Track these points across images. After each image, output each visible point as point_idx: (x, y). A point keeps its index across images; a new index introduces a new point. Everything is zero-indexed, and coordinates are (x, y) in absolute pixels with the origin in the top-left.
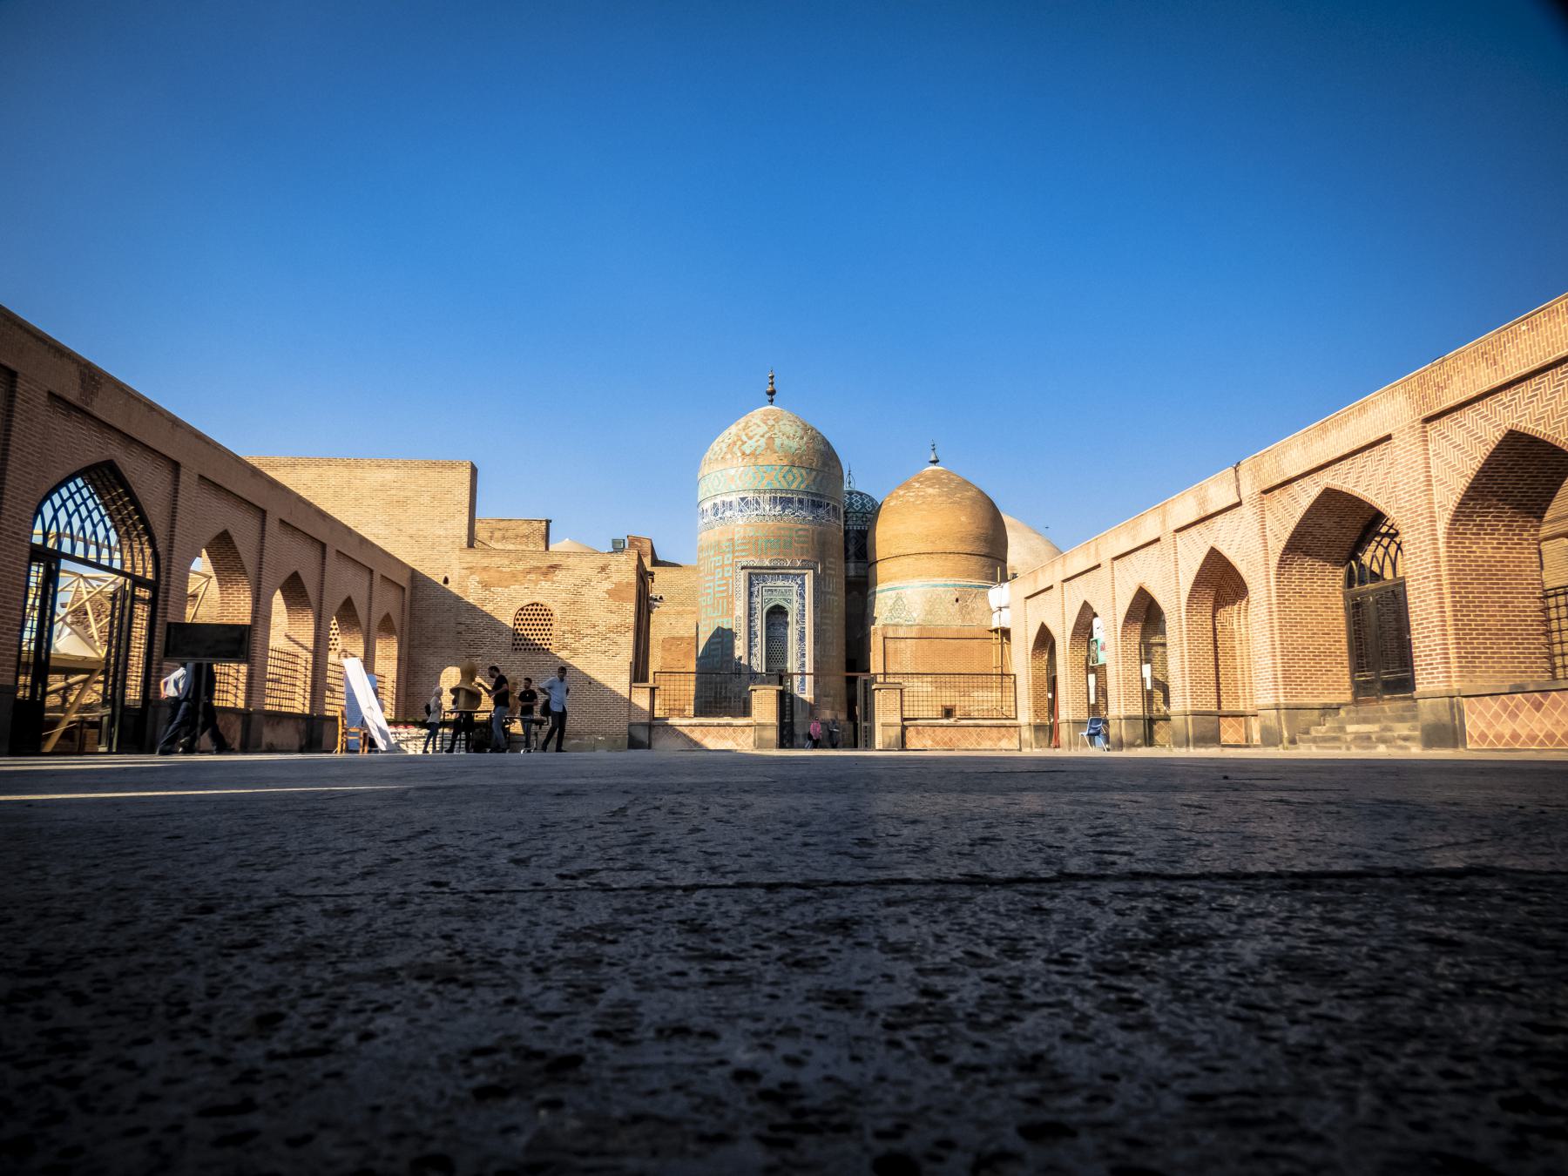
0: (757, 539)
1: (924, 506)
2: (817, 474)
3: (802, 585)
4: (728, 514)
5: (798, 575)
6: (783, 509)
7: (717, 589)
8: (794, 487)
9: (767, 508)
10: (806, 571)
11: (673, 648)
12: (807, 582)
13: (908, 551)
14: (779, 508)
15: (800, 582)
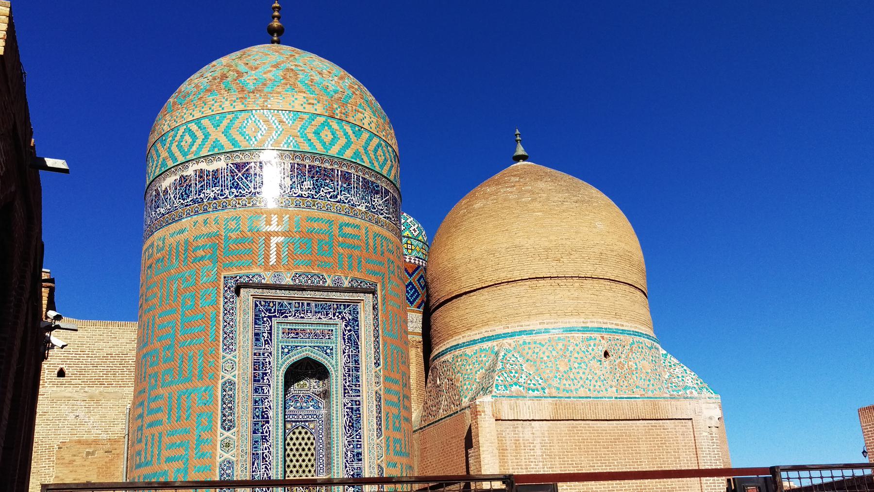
1: (537, 205)
2: (370, 140)
3: (353, 323)
4: (210, 192)
6: (317, 187)
8: (334, 151)
10: (361, 296)
11: (79, 461)
12: (362, 317)
13: (517, 275)
14: (308, 184)
15: (348, 317)
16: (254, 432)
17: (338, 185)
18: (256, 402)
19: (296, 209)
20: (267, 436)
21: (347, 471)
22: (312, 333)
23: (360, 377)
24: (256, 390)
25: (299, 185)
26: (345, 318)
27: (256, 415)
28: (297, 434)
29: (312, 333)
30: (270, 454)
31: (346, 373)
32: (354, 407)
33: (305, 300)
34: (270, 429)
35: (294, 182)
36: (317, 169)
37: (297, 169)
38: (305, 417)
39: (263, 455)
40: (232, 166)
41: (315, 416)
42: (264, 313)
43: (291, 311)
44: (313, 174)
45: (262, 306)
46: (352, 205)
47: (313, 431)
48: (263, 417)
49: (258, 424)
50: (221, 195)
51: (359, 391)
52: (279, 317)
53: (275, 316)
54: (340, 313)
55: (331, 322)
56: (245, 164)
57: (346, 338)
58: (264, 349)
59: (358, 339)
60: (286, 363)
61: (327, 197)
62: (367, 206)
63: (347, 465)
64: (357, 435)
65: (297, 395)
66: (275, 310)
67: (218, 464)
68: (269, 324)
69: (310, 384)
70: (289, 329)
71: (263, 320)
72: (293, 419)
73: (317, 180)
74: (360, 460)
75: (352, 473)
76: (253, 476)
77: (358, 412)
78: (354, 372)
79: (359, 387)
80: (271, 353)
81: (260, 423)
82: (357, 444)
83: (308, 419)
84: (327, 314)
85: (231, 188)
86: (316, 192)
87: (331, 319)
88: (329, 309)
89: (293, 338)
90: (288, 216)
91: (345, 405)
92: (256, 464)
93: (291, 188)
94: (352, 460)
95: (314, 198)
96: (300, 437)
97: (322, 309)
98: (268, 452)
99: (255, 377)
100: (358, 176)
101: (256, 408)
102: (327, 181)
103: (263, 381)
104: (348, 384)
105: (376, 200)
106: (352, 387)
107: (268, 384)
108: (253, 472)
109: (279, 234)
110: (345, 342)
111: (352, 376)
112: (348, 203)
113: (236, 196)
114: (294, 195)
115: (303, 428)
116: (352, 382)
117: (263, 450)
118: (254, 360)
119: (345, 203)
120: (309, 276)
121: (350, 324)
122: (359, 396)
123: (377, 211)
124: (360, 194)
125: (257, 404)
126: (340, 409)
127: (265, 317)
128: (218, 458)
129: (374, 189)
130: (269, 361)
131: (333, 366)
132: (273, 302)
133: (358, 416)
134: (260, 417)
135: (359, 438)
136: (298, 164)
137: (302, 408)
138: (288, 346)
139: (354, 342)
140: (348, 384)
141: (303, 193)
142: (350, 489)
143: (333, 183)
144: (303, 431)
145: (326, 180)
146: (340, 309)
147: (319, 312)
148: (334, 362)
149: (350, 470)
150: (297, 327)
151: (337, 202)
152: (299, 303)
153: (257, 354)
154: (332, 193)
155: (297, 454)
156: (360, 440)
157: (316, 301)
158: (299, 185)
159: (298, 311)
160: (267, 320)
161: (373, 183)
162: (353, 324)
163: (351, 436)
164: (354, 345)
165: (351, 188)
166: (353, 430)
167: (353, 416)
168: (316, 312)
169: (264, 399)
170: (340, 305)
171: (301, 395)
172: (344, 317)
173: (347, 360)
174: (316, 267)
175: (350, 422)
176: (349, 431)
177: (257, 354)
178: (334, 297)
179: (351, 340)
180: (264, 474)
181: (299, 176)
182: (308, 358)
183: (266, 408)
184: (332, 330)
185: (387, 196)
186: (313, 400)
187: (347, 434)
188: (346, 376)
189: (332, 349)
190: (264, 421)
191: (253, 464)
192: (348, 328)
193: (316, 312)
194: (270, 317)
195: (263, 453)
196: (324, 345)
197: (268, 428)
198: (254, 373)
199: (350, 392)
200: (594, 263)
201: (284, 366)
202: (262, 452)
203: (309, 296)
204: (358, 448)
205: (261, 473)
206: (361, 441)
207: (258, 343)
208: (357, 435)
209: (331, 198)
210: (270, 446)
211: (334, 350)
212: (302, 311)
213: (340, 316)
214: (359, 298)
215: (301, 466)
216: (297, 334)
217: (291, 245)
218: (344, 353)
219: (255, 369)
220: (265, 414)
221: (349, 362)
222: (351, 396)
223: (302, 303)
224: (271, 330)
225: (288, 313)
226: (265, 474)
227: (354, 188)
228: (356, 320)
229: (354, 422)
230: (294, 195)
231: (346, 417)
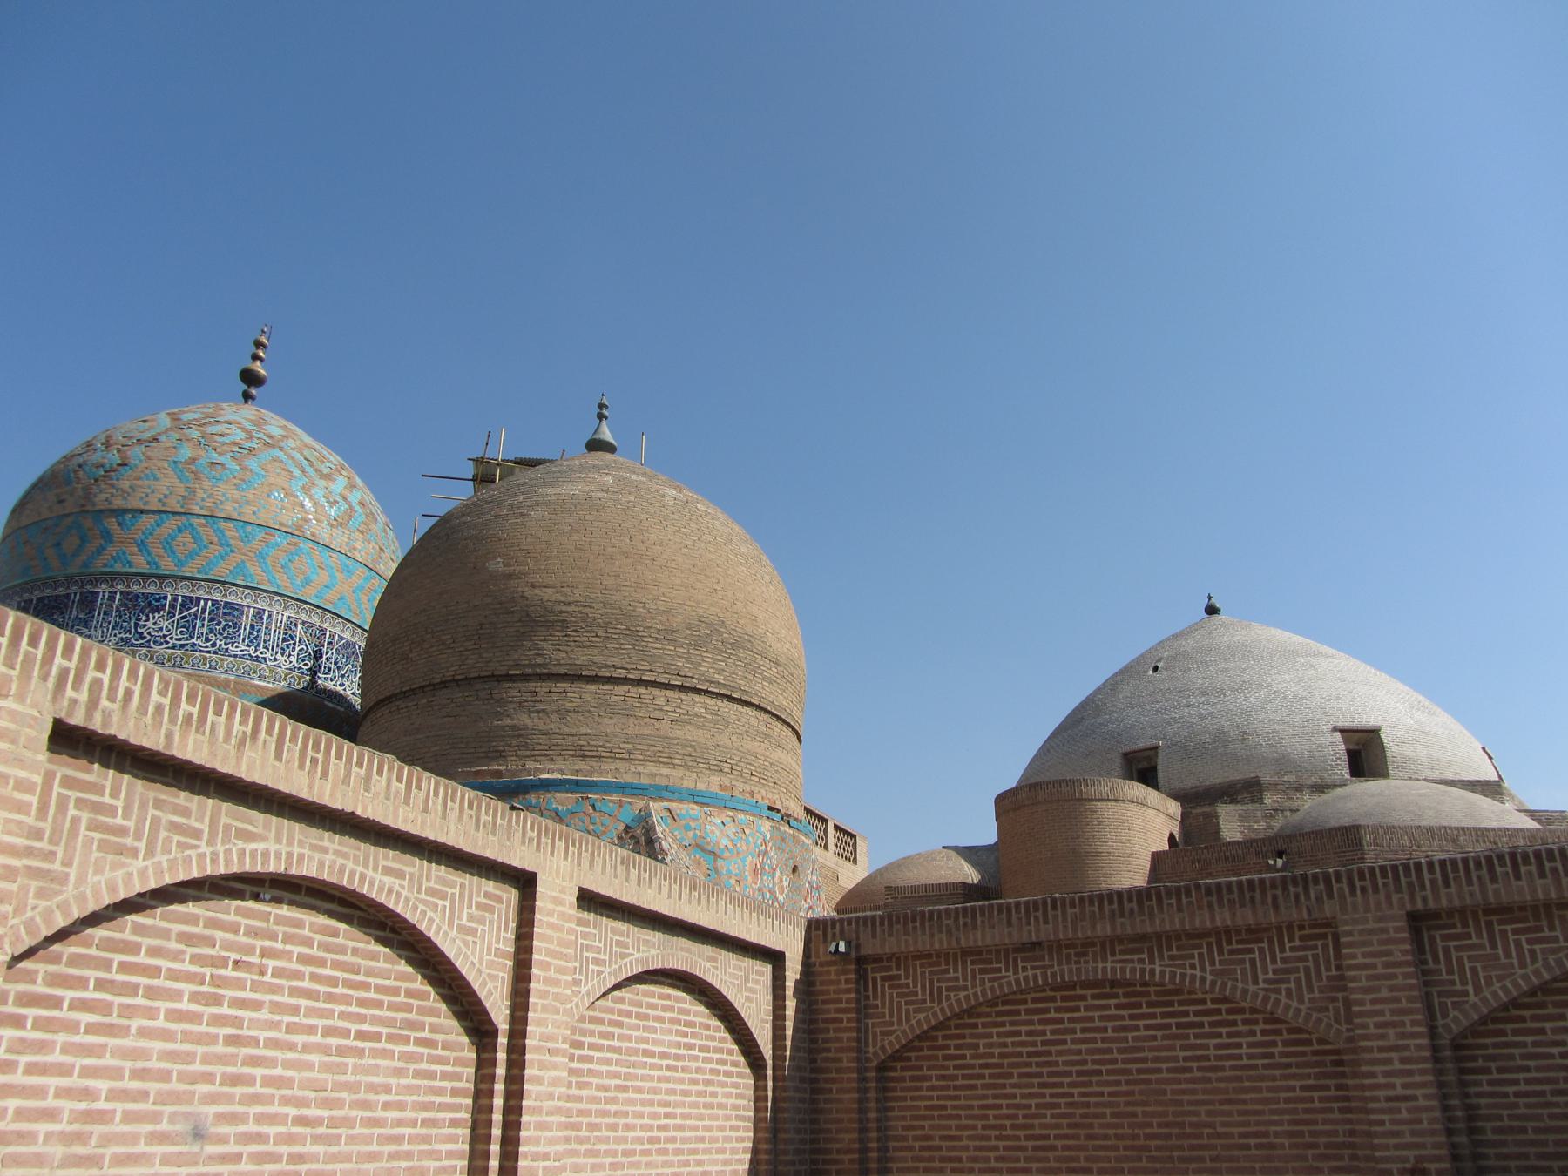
36: (46, 602)
62: (122, 639)
102: (55, 617)
105: (150, 624)
123: (149, 641)
124: (109, 623)
129: (150, 603)
165: (93, 617)
200: (461, 649)
227: (99, 614)
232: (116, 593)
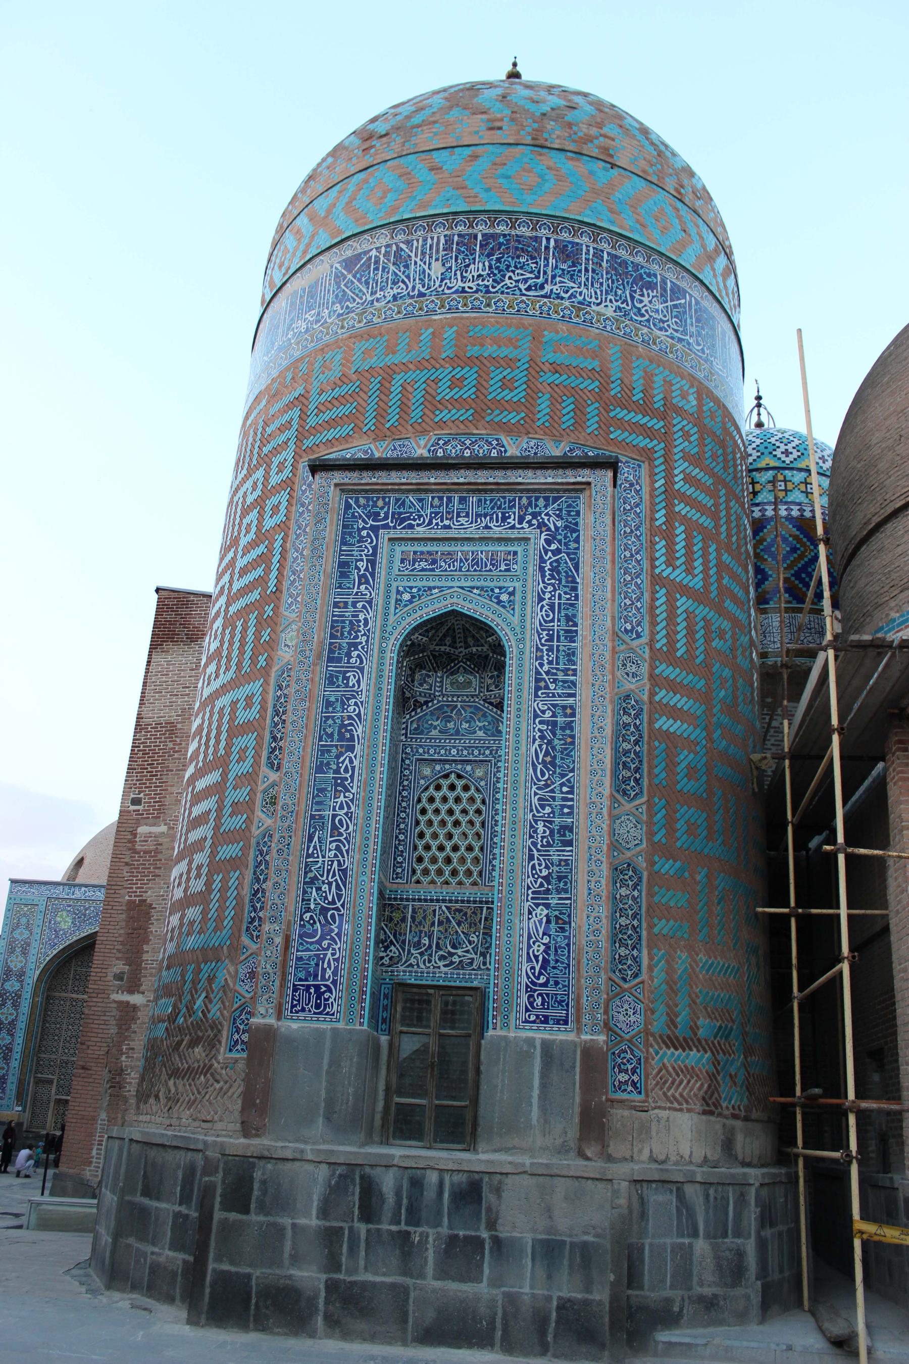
0: (389, 372)
5: (552, 493)
6: (497, 273)
7: (236, 586)
9: (436, 270)
10: (584, 475)
16: (319, 769)
17: (546, 266)
18: (329, 704)
19: (448, 316)
20: (346, 779)
21: (533, 867)
22: (467, 560)
23: (579, 652)
24: (331, 680)
25: (458, 273)
26: (546, 525)
27: (326, 733)
28: (445, 789)
29: (467, 560)
30: (350, 819)
31: (543, 645)
32: (560, 720)
33: (456, 491)
34: (356, 763)
35: (450, 268)
36: (501, 240)
37: (458, 244)
38: (465, 752)
39: (333, 820)
40: (338, 266)
41: (487, 752)
42: (364, 521)
43: (420, 516)
44: (492, 249)
45: (359, 507)
46: (579, 303)
47: (483, 783)
48: (341, 737)
49: (329, 751)
50: (317, 321)
51: (575, 685)
52: (395, 527)
53: (386, 527)
54: (535, 515)
55: (514, 534)
56: (358, 257)
57: (548, 566)
58: (357, 594)
59: (577, 570)
60: (404, 623)
61: (520, 290)
62: (619, 308)
63: (535, 852)
64: (562, 785)
65: (448, 706)
66: (387, 514)
67: (253, 841)
68: (372, 542)
69: (481, 682)
70: (415, 553)
71: (359, 535)
72: (436, 757)
73: (498, 260)
74: (570, 843)
75: (545, 873)
76: (306, 866)
77: (568, 732)
78: (564, 643)
79: (575, 675)
80: (370, 602)
81: (334, 750)
82: (563, 807)
83: (471, 758)
84: (504, 519)
85: (333, 303)
86: (494, 281)
87: (513, 527)
88: (510, 508)
89: (423, 570)
90: (431, 330)
91: (536, 716)
92: (316, 839)
93: (442, 280)
94: (548, 842)
95: (490, 292)
96: (451, 796)
97: (492, 508)
98: (346, 814)
99: (331, 651)
100: (598, 254)
101: (327, 718)
103: (348, 662)
104: (546, 668)
106: (556, 674)
107: (358, 668)
108: (308, 856)
109: (411, 366)
110: (543, 576)
111: (558, 651)
112: (569, 298)
113: (340, 315)
114: (446, 291)
115: (459, 777)
116: (558, 664)
117: (334, 810)
118: (333, 616)
119: (562, 298)
120: (468, 442)
121: (559, 537)
122: (574, 695)
123: (648, 321)
124: (602, 284)
125: (331, 709)
126: (524, 726)
127: (364, 528)
128: (253, 829)
129: (642, 278)
130: (366, 620)
131: (513, 629)
132: (384, 498)
133: (569, 740)
134: (336, 736)
135: (567, 793)
136: (459, 235)
137: (457, 732)
138: (411, 588)
139: (567, 576)
140: (546, 668)
141: (466, 285)
142: (538, 911)
143: (536, 263)
144: (459, 784)
145: (518, 257)
146: (536, 506)
147: (485, 516)
148: (516, 620)
149: (540, 865)
150: (435, 549)
151: (542, 296)
152: (441, 499)
153: (342, 605)
154: (530, 282)
155: (442, 833)
156: (570, 796)
157: (479, 491)
158: (458, 273)
159: (436, 514)
160: (368, 535)
161: (636, 266)
162: (566, 537)
163: (547, 786)
164: (567, 582)
165: (580, 271)
166: (554, 772)
167: (556, 742)
168: (478, 515)
169: (348, 699)
170: (537, 499)
171: (459, 704)
172: (543, 522)
173: (547, 616)
174: (480, 425)
175: (547, 753)
176: (543, 774)
177: (342, 605)
178: (520, 480)
179: (559, 573)
180: (333, 862)
181: (460, 257)
182: (454, 614)
183: (350, 718)
184: (515, 553)
185: (678, 299)
186: (484, 716)
187: (539, 780)
188: (542, 651)
189: (512, 594)
190: (342, 746)
191: (311, 839)
192: (553, 547)
193: (478, 515)
194: (375, 529)
195: (334, 816)
196: (492, 585)
197: (351, 761)
198: (331, 644)
199: (552, 686)
201: (399, 629)
202: (331, 812)
203: (462, 480)
204: (563, 814)
205: (327, 859)
206: (572, 800)
207: (345, 582)
208: (562, 785)
209: (527, 290)
210: (352, 800)
211: (518, 597)
212: (448, 513)
213: (534, 522)
214: (579, 479)
215: (448, 860)
216: (434, 562)
217: (432, 384)
218: (541, 599)
219: (333, 636)
220: (347, 731)
221: (552, 621)
222: (554, 696)
223: (449, 499)
224: (375, 553)
225: (414, 520)
226: (336, 863)
227: (587, 270)
228: (573, 528)
229: (559, 755)
230: (446, 291)
231: (537, 743)
232: (602, 251)
